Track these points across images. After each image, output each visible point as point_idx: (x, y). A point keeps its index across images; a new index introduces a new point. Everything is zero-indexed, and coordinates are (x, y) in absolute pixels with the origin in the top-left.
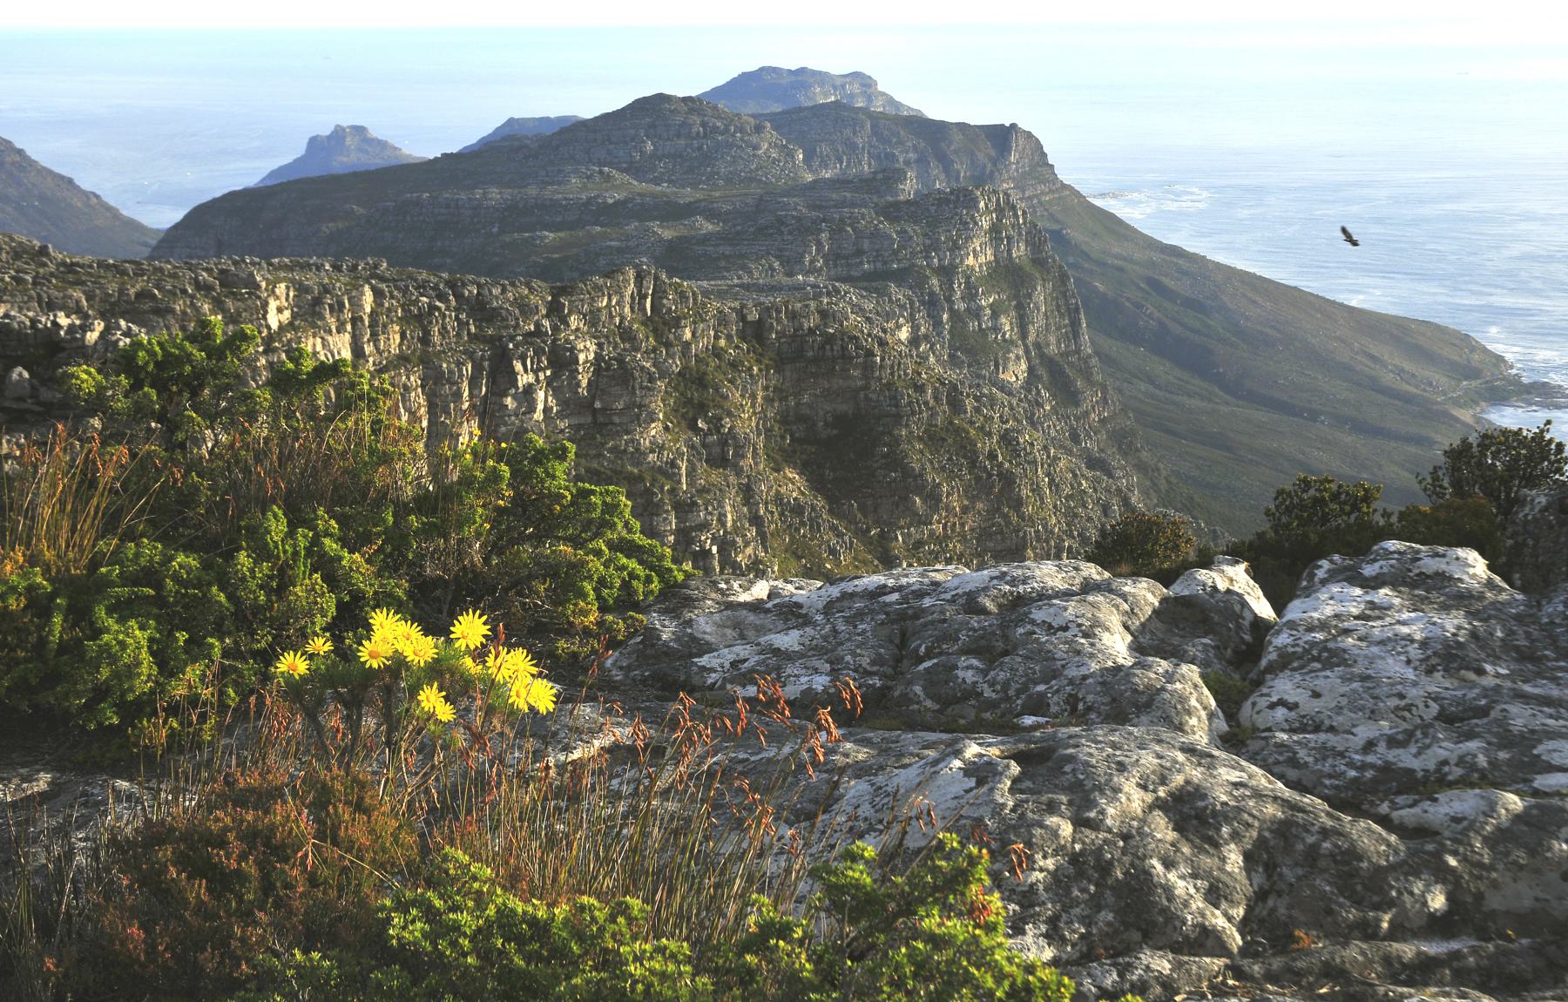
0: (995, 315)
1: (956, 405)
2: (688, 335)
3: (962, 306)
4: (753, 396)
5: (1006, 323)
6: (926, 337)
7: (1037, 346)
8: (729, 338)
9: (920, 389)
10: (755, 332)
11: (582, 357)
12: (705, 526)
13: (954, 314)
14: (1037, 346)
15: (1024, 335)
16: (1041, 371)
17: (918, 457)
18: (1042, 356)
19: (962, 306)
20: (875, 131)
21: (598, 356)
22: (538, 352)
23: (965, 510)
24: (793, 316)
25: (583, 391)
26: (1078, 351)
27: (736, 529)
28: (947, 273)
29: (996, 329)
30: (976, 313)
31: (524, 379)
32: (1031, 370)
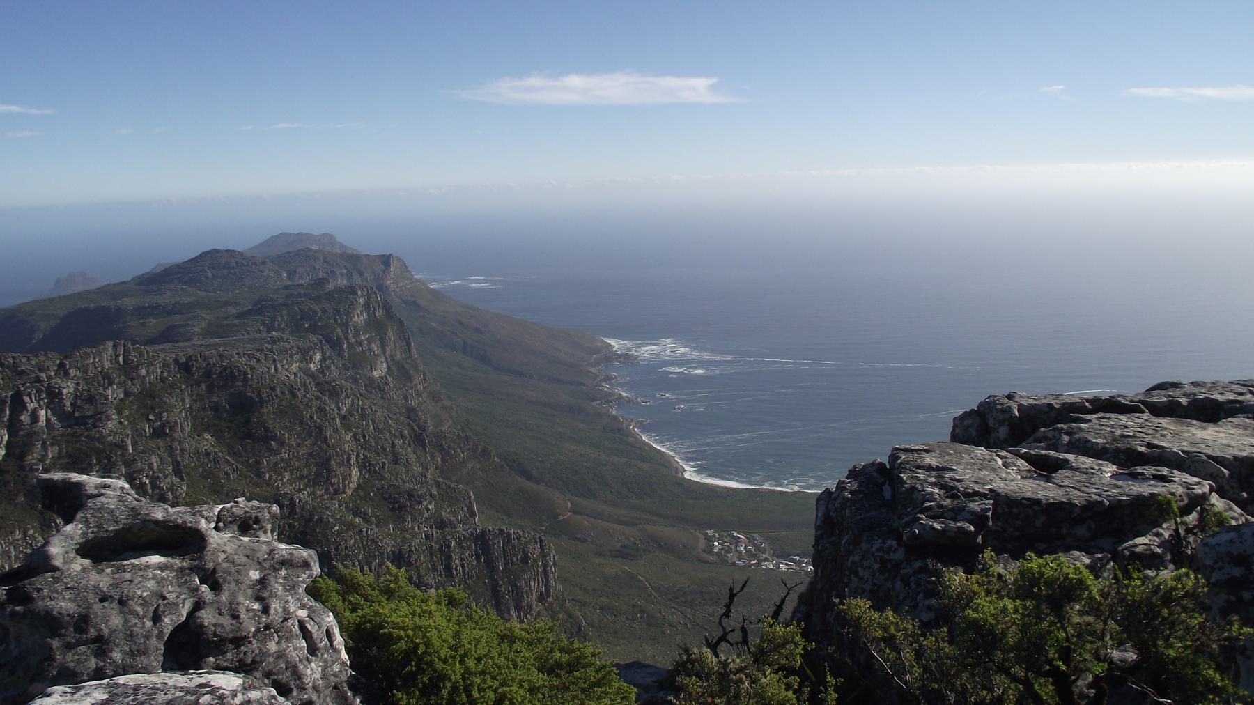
0: (369, 343)
1: (293, 394)
2: (144, 372)
3: (353, 340)
4: (183, 400)
5: (375, 347)
6: (330, 358)
7: (391, 356)
8: (169, 372)
9: (273, 389)
10: (186, 368)
11: (65, 391)
12: (141, 471)
13: (349, 344)
14: (391, 356)
15: (384, 352)
16: (393, 368)
17: (273, 424)
18: (393, 360)
19: (353, 340)
20: (325, 261)
21: (76, 390)
22: (39, 391)
23: (298, 445)
24: (205, 358)
25: (69, 408)
26: (411, 356)
27: (160, 470)
28: (345, 326)
29: (370, 350)
30: (360, 344)
31: (31, 406)
32: (389, 368)
